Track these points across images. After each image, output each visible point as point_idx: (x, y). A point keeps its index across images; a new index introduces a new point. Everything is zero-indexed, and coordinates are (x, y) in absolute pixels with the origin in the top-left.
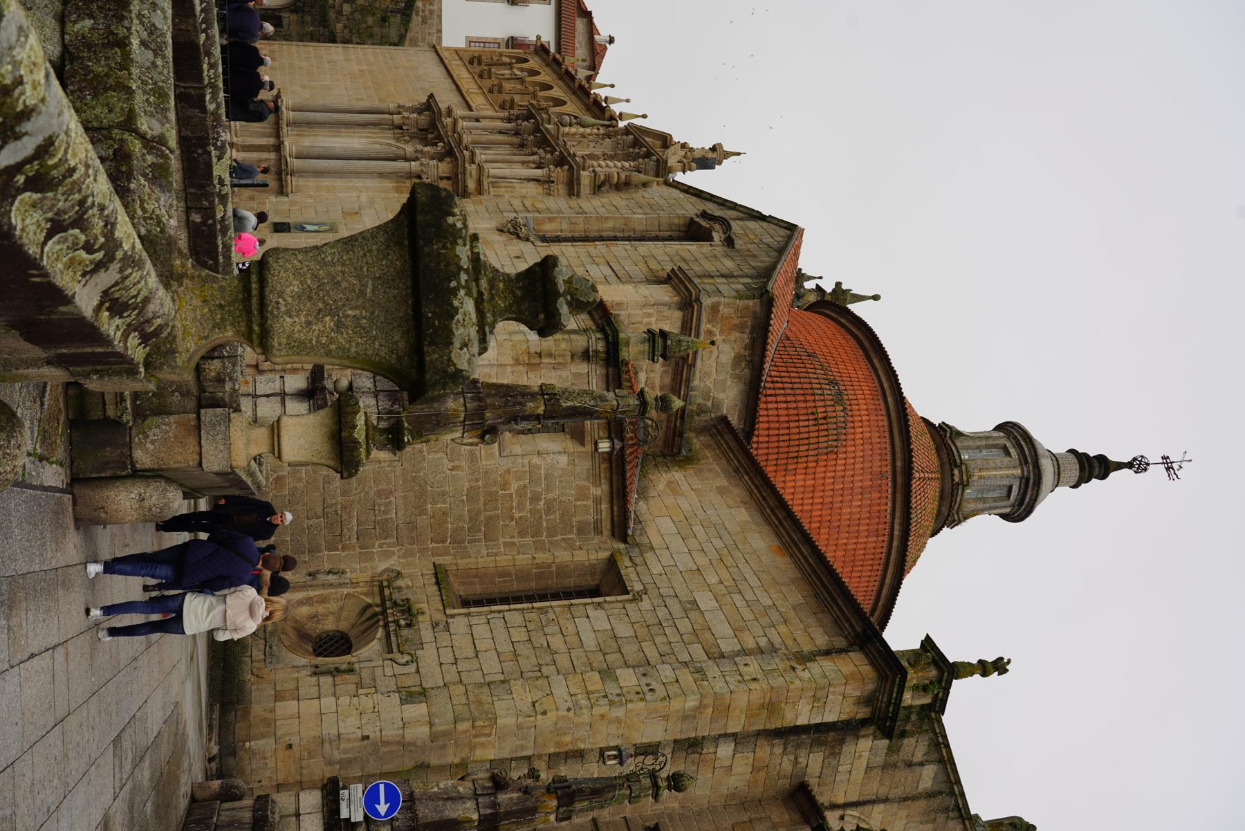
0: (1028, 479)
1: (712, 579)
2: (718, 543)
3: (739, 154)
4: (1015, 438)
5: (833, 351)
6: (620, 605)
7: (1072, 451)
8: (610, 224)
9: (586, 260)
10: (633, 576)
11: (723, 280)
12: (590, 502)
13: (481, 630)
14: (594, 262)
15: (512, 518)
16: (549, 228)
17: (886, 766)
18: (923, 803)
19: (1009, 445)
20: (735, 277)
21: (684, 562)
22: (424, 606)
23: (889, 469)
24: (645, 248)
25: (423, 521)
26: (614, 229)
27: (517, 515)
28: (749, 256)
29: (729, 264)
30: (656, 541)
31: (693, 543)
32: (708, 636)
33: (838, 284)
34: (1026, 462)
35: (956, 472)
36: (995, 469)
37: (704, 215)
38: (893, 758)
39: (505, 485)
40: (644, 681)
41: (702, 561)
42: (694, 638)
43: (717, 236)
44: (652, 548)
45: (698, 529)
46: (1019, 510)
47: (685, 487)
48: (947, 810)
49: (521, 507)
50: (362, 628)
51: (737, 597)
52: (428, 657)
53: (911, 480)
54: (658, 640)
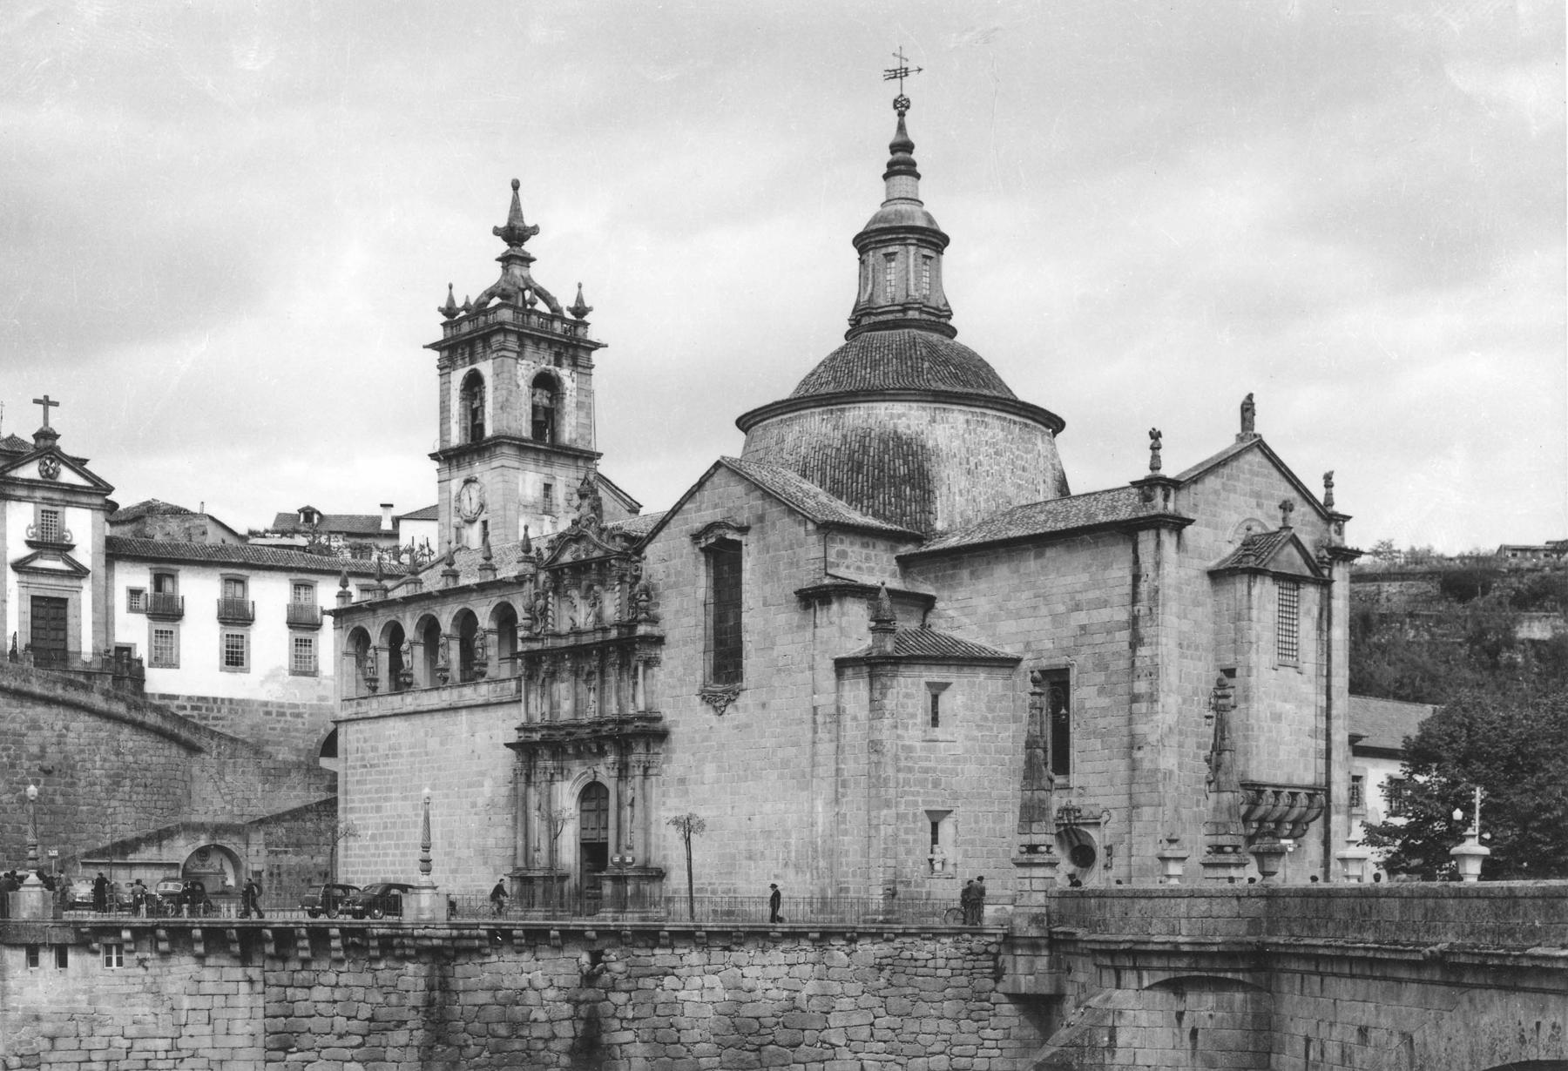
0: (918, 240)
4: (877, 242)
7: (886, 177)
19: (884, 251)
22: (1064, 804)
33: (496, 231)
34: (905, 239)
35: (912, 314)
39: (974, 739)
46: (934, 240)
52: (1104, 802)
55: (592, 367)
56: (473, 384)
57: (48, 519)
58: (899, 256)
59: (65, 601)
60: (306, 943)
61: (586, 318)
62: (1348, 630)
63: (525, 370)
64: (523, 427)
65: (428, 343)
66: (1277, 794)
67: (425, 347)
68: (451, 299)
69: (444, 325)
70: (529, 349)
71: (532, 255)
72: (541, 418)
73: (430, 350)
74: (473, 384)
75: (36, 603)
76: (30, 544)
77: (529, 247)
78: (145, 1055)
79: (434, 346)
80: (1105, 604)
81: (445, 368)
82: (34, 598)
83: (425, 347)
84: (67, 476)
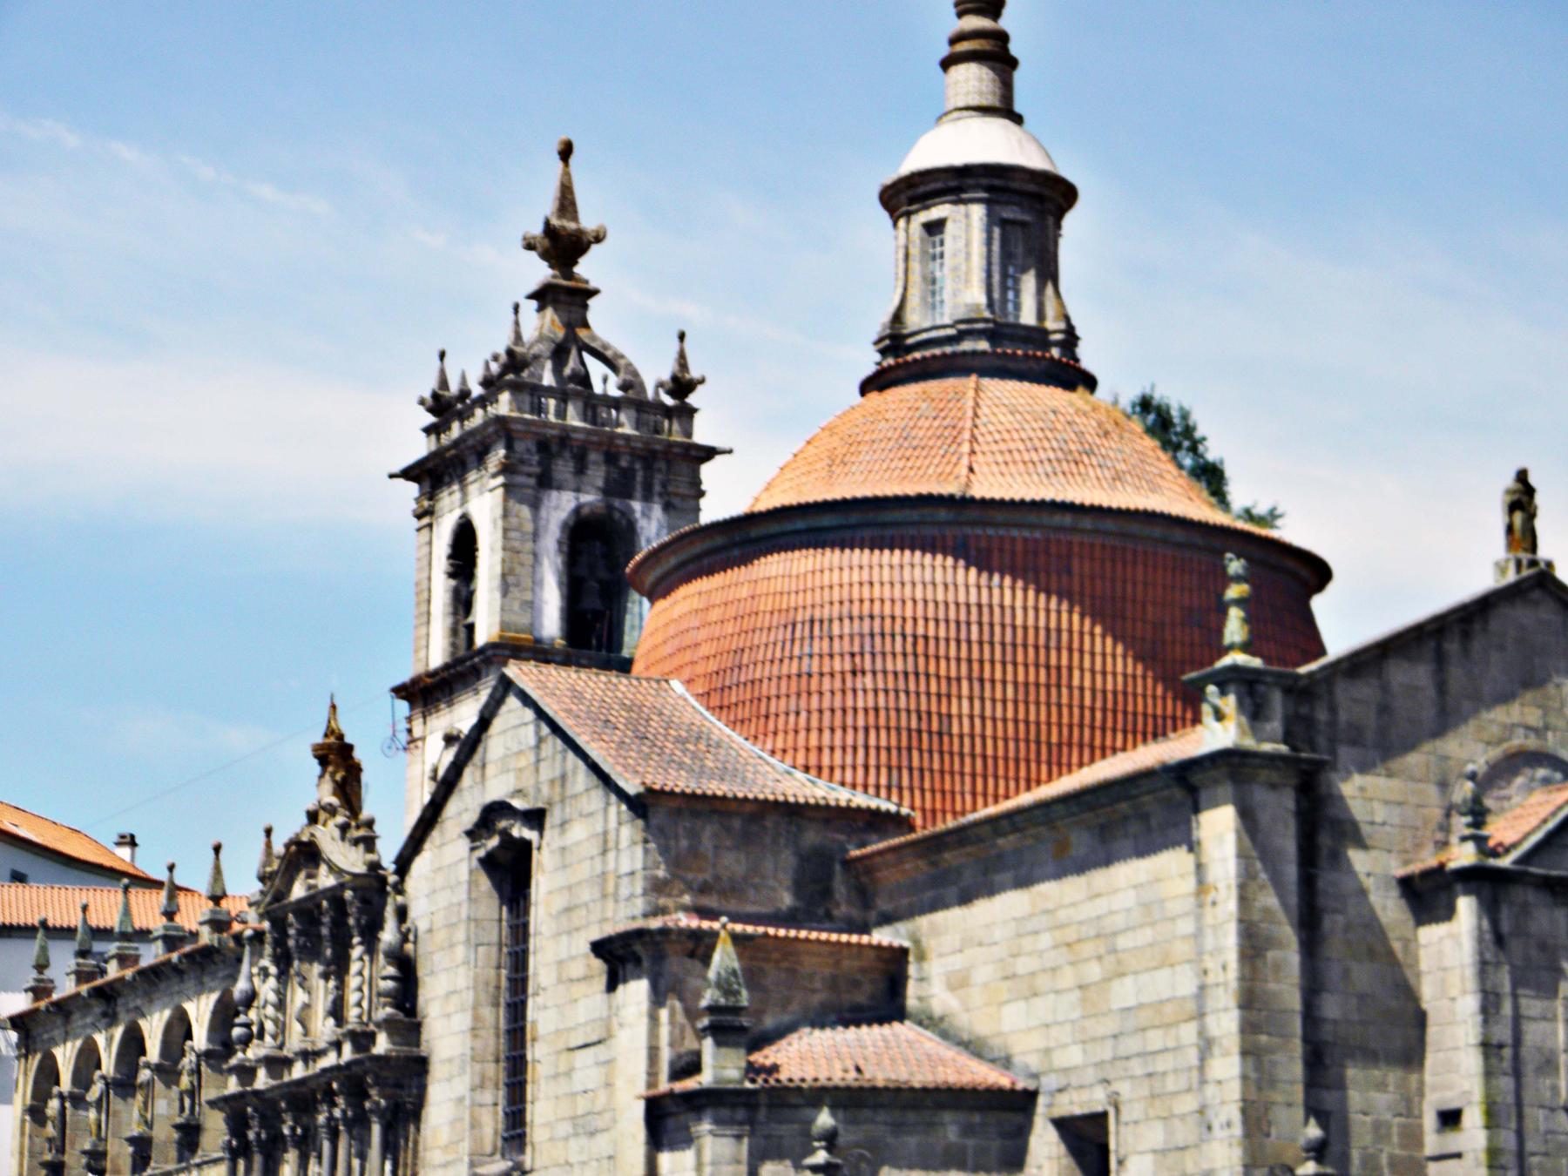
1: (1094, 971)
2: (1045, 940)
3: (334, 707)
5: (731, 611)
6: (1123, 1129)
8: (487, 1013)
9: (563, 1087)
10: (1084, 1096)
11: (611, 855)
12: (970, 1142)
14: (569, 1073)
16: (492, 1124)
18: (1456, 674)
20: (605, 833)
21: (1068, 1006)
23: (948, 532)
24: (541, 967)
26: (496, 1005)
28: (563, 785)
29: (578, 832)
30: (1037, 1041)
31: (1043, 982)
32: (1169, 1009)
35: (967, 346)
36: (968, 256)
37: (473, 834)
38: (1370, 735)
40: (1217, 1132)
41: (1067, 978)
42: (1173, 1031)
43: (519, 831)
44: (1047, 1051)
45: (1023, 966)
47: (957, 962)
48: (1466, 636)
51: (1123, 942)
53: (972, 499)
54: (1171, 1084)
55: (702, 494)
56: (465, 541)
61: (692, 400)
62: (424, 1113)
63: (561, 506)
64: (551, 624)
65: (397, 469)
67: (392, 476)
68: (444, 383)
69: (428, 430)
70: (563, 468)
71: (593, 284)
72: (592, 602)
73: (401, 481)
74: (465, 541)
77: (587, 268)
79: (408, 474)
80: (1166, 962)
81: (425, 514)
83: (392, 476)
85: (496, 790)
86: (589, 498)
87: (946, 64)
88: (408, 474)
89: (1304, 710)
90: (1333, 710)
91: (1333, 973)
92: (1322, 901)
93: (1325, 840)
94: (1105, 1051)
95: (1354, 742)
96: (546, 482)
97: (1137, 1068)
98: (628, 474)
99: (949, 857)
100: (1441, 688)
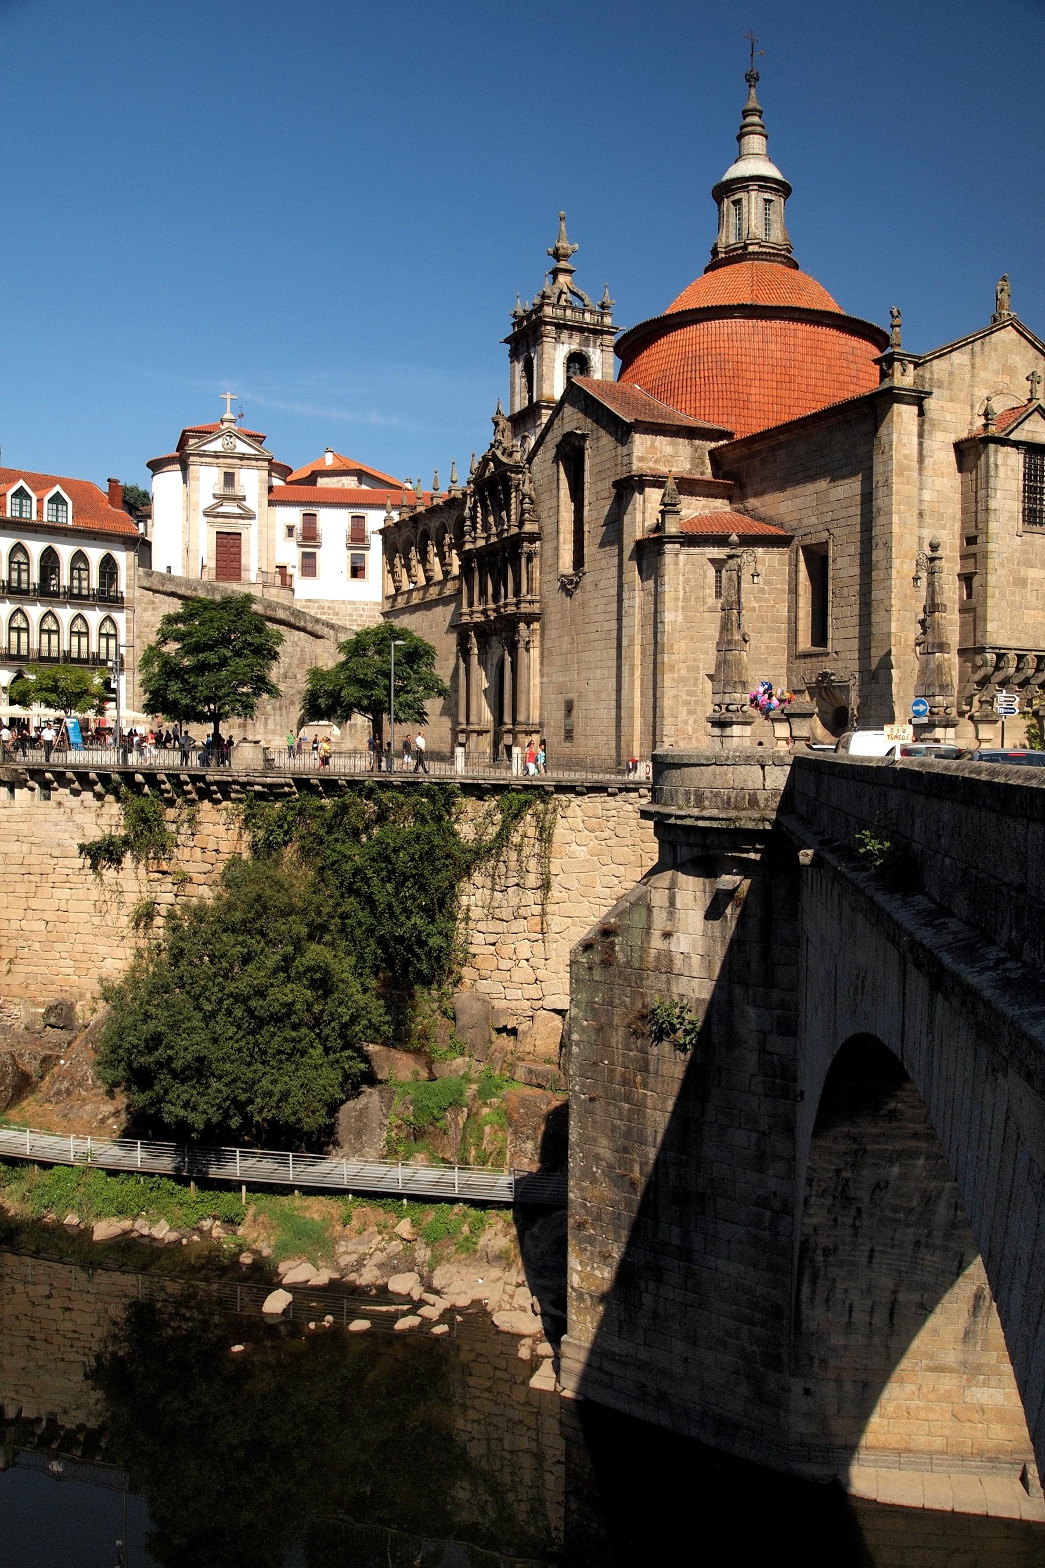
0: (759, 186)
13: (842, 633)
15: (774, 606)
17: (950, 388)
19: (732, 199)
25: (772, 660)
27: (772, 603)
30: (795, 515)
34: (747, 186)
35: (751, 249)
38: (946, 384)
44: (800, 520)
49: (767, 600)
50: (833, 700)
57: (229, 479)
58: (744, 203)
59: (240, 534)
60: (168, 786)
66: (1020, 658)
69: (513, 325)
75: (220, 536)
76: (215, 496)
78: (66, 871)
79: (506, 341)
82: (218, 533)
84: (242, 448)
85: (567, 429)
86: (574, 347)
87: (740, 138)
88: (506, 341)
89: (921, 373)
90: (932, 372)
91: (928, 481)
92: (925, 453)
93: (926, 427)
94: (828, 517)
95: (940, 387)
96: (557, 340)
97: (843, 522)
98: (587, 339)
99: (757, 446)
100: (973, 366)
